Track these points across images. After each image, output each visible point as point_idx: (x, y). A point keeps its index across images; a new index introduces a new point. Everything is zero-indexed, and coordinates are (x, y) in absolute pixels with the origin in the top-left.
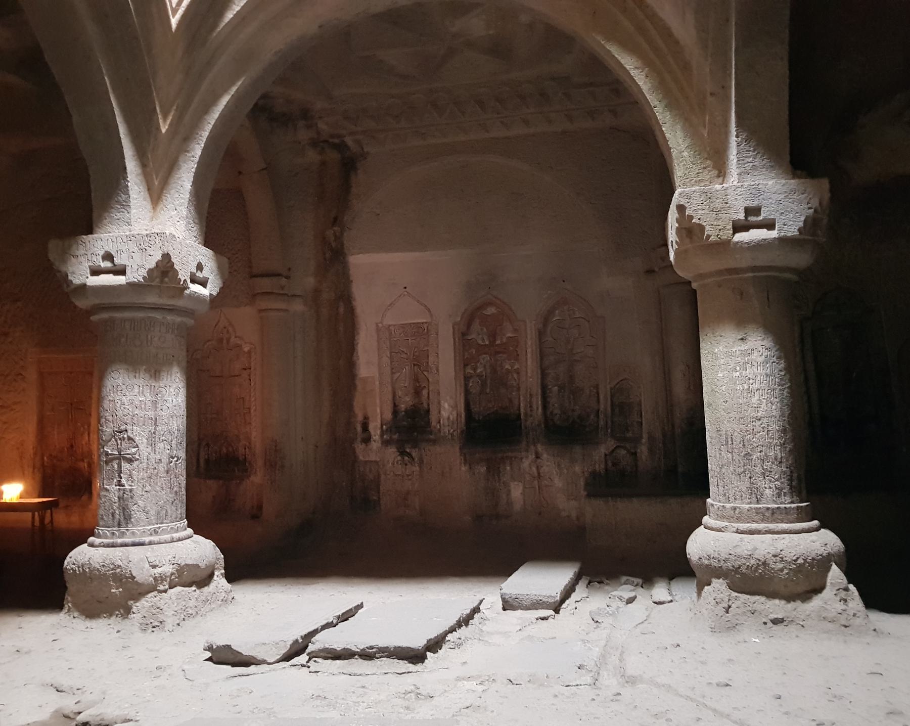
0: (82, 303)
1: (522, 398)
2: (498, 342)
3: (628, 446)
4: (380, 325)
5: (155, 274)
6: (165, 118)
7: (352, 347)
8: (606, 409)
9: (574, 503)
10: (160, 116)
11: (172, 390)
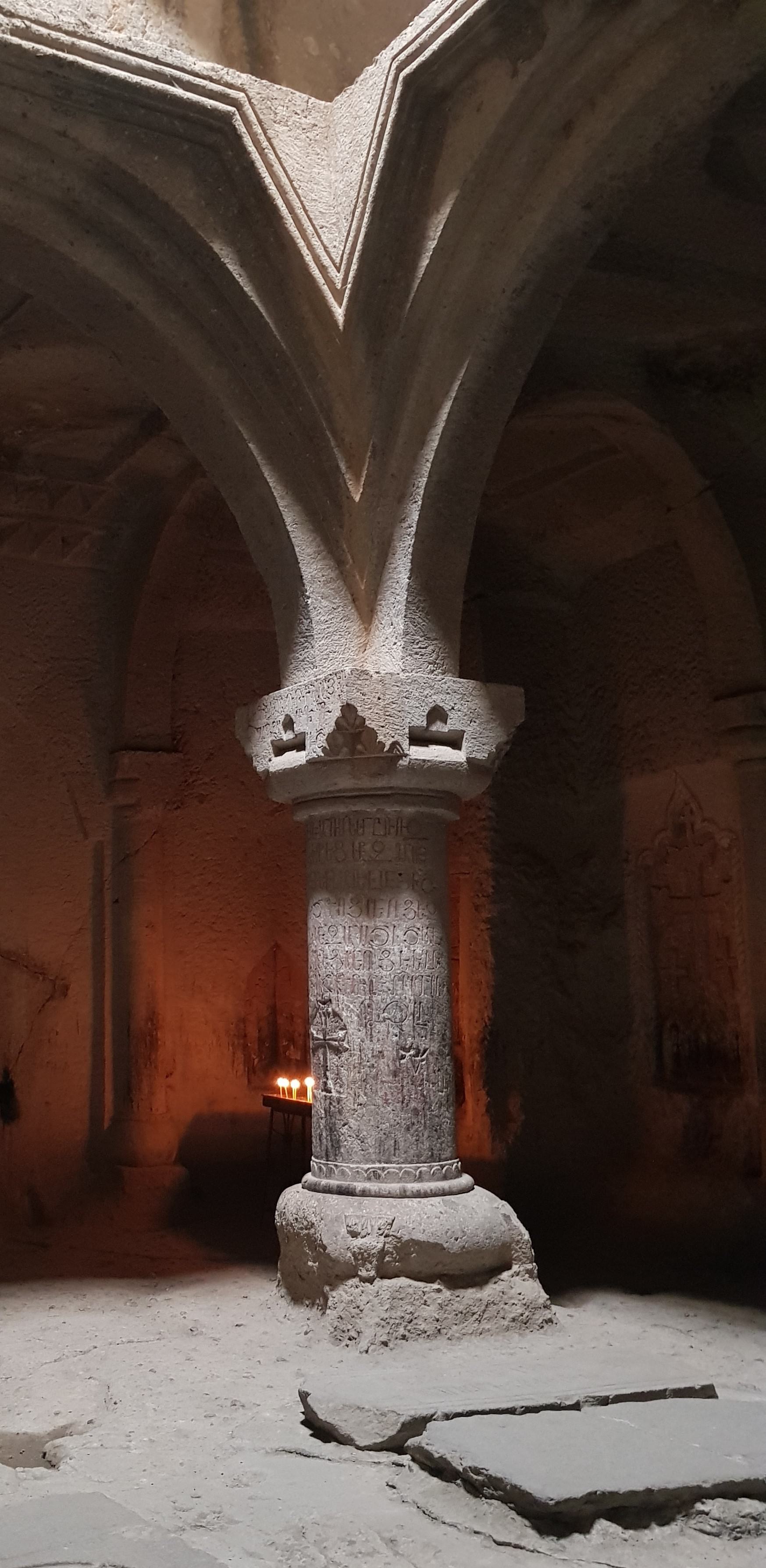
0: (280, 796)
5: (340, 740)
6: (357, 477)
10: (347, 476)
11: (399, 932)
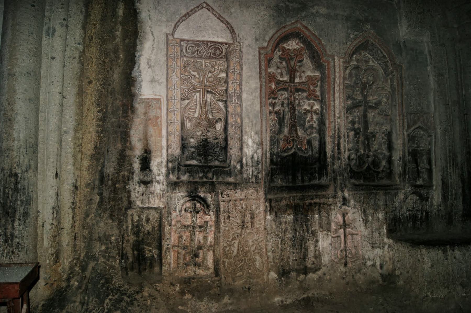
1: (328, 140)
2: (297, 80)
3: (423, 192)
4: (171, 38)
7: (131, 61)
8: (404, 155)
9: (378, 251)
